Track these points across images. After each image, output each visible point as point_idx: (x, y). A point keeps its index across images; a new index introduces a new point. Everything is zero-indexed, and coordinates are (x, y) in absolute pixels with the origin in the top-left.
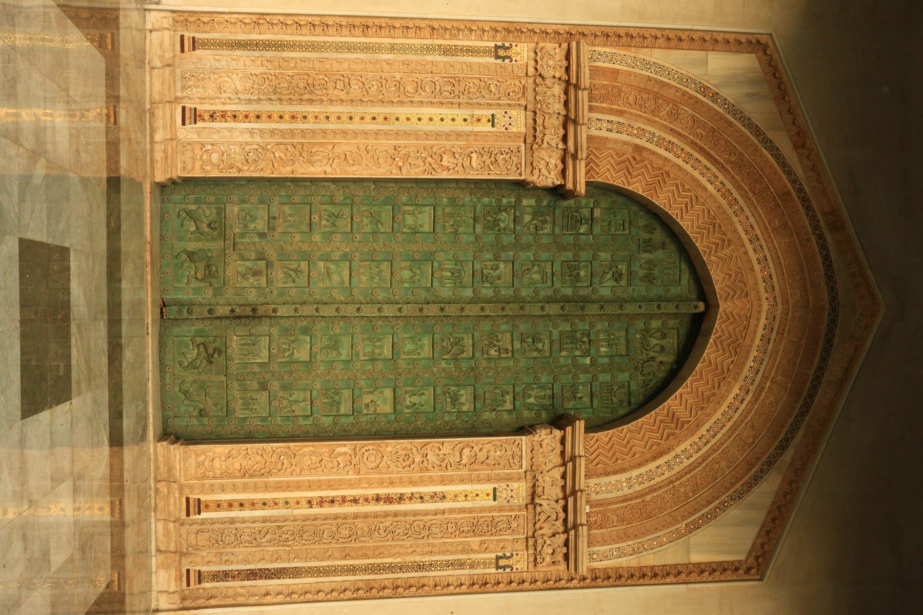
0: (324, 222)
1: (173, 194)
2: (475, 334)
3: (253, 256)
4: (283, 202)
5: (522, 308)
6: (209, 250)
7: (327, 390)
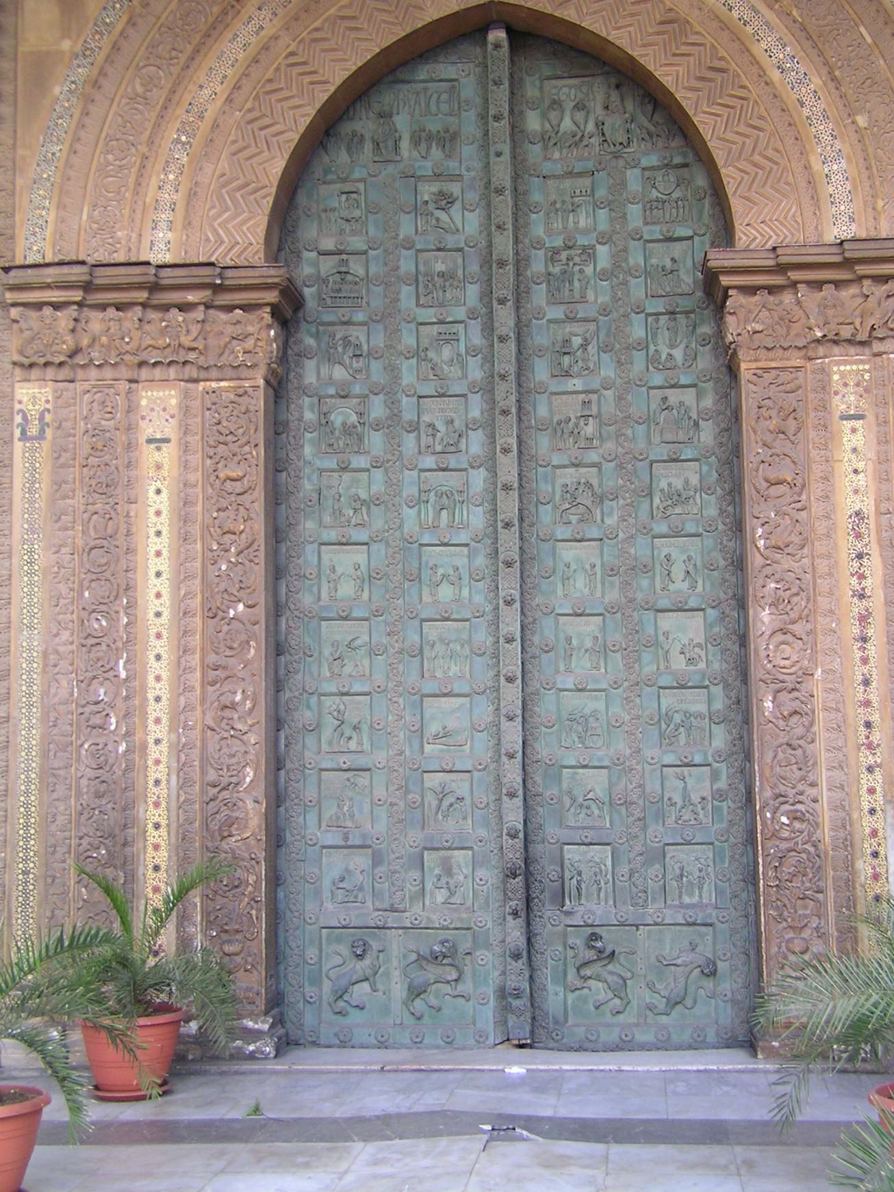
0: (353, 745)
1: (302, 1025)
2: (555, 462)
3: (416, 874)
4: (315, 819)
5: (503, 377)
6: (404, 956)
7: (661, 735)
